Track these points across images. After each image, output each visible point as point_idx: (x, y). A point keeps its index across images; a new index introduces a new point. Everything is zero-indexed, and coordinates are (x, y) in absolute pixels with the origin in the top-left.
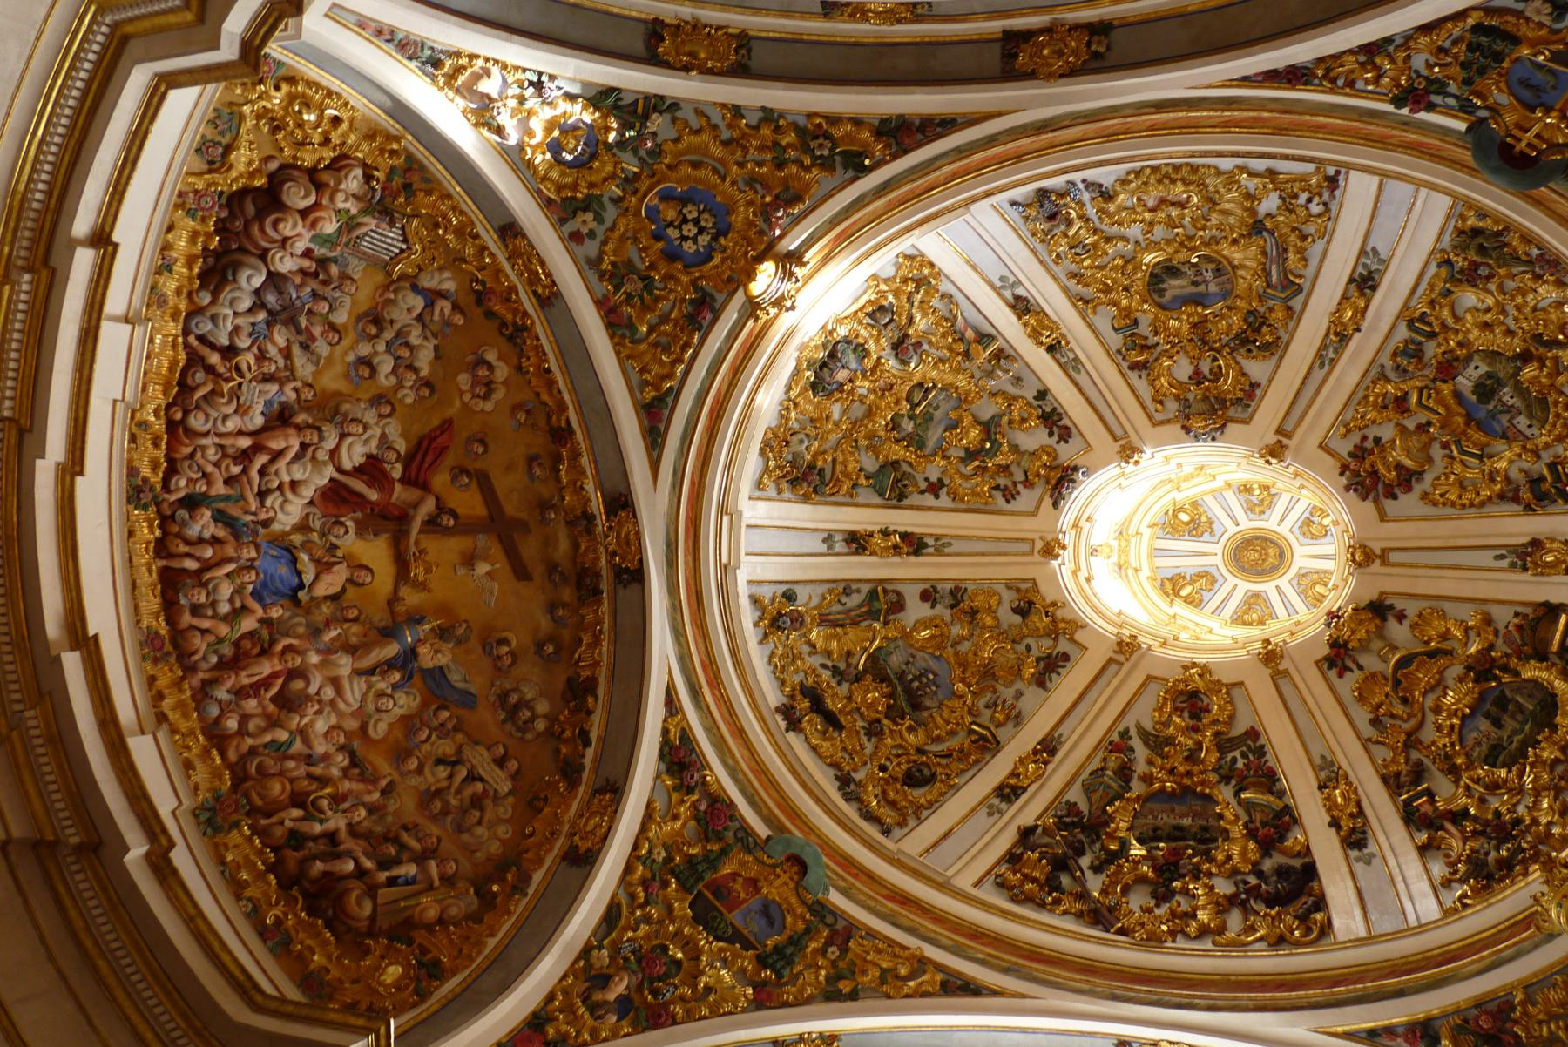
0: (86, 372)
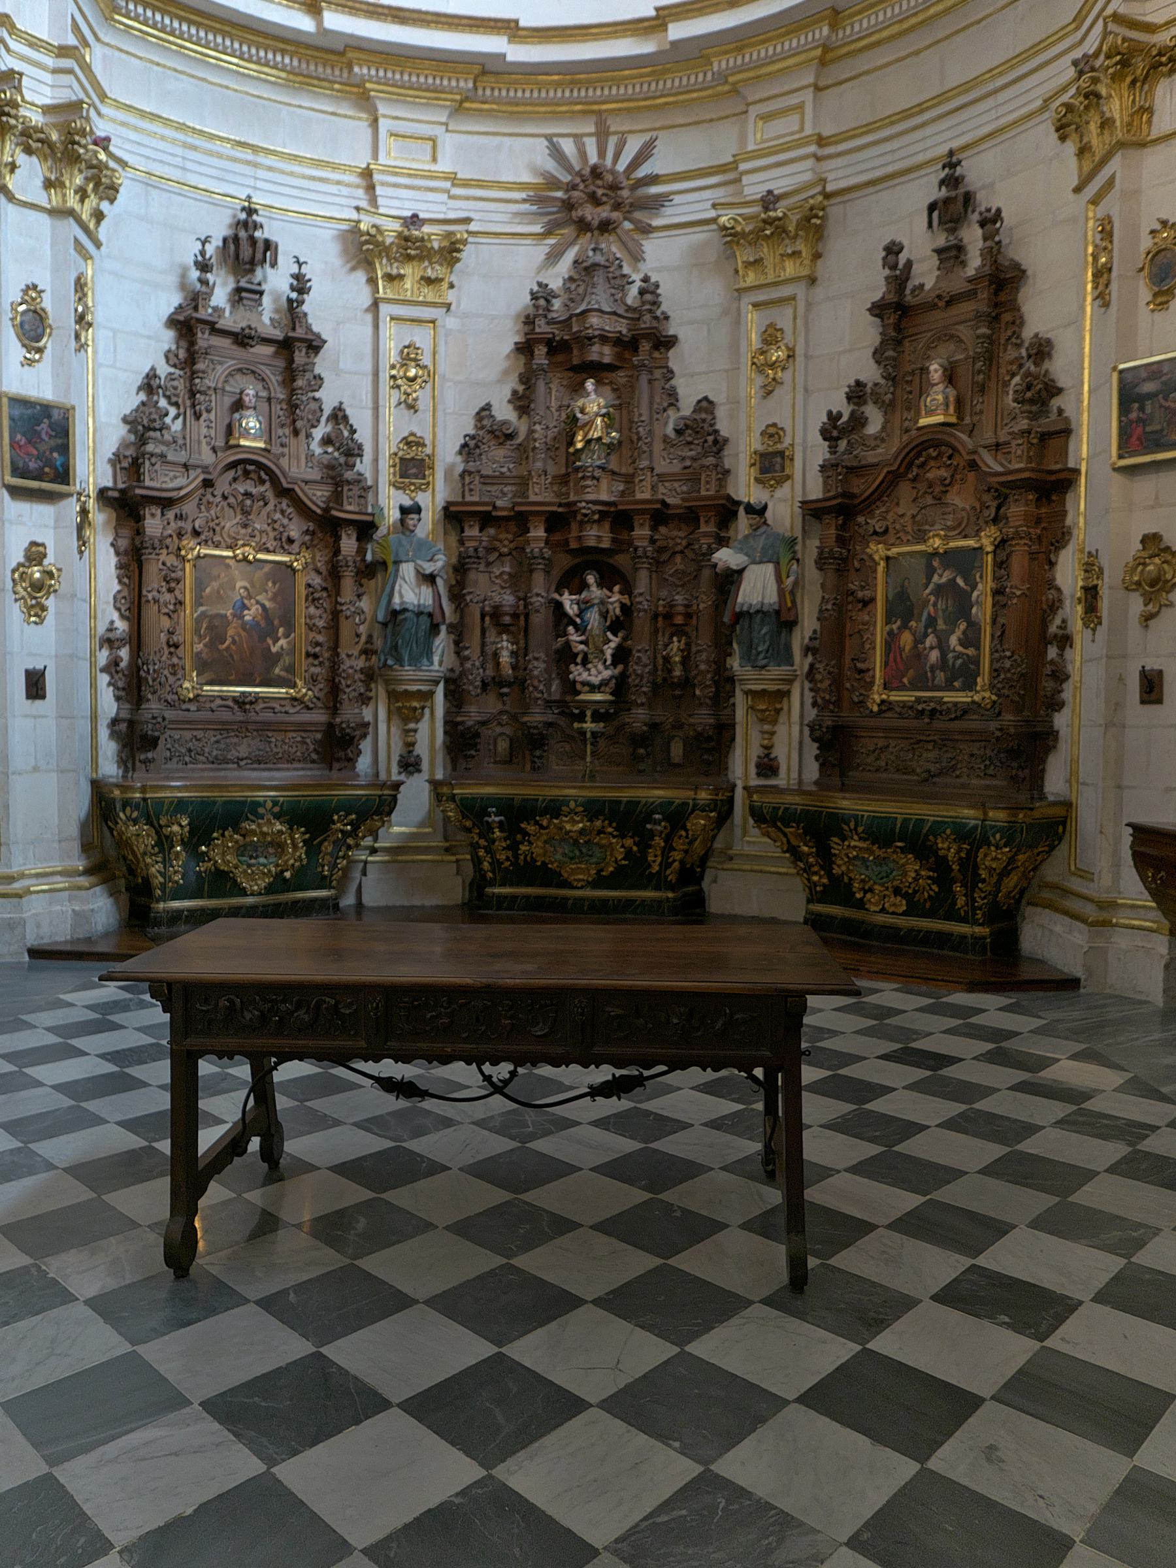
0: (429, 18)
